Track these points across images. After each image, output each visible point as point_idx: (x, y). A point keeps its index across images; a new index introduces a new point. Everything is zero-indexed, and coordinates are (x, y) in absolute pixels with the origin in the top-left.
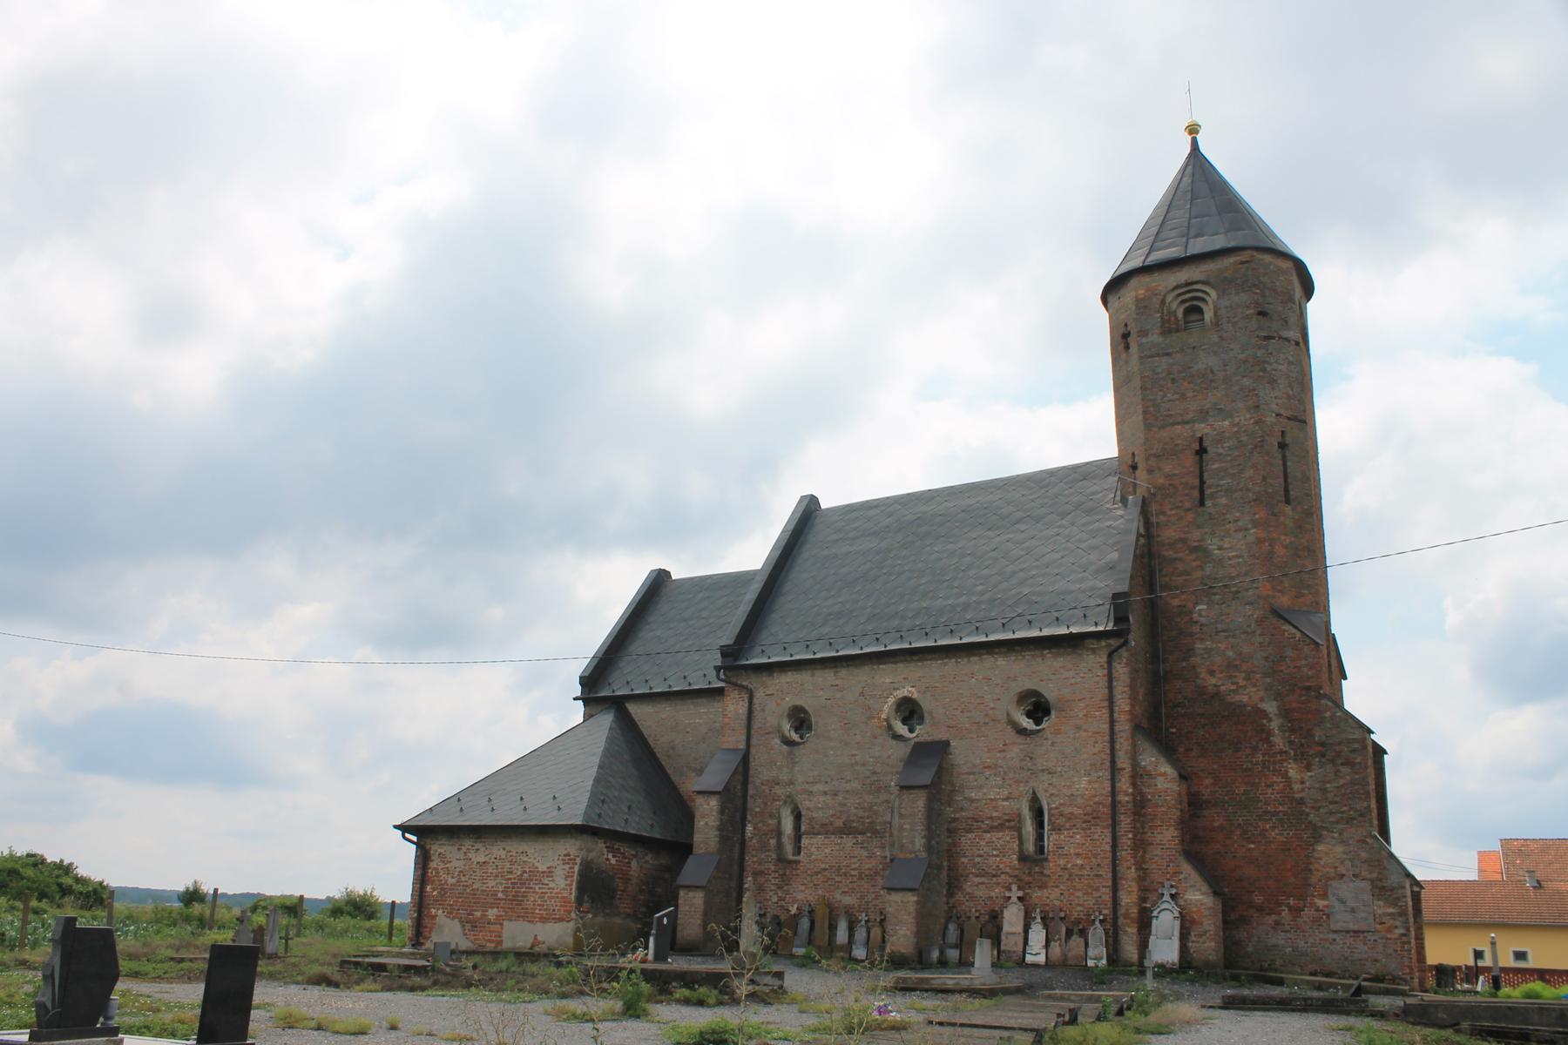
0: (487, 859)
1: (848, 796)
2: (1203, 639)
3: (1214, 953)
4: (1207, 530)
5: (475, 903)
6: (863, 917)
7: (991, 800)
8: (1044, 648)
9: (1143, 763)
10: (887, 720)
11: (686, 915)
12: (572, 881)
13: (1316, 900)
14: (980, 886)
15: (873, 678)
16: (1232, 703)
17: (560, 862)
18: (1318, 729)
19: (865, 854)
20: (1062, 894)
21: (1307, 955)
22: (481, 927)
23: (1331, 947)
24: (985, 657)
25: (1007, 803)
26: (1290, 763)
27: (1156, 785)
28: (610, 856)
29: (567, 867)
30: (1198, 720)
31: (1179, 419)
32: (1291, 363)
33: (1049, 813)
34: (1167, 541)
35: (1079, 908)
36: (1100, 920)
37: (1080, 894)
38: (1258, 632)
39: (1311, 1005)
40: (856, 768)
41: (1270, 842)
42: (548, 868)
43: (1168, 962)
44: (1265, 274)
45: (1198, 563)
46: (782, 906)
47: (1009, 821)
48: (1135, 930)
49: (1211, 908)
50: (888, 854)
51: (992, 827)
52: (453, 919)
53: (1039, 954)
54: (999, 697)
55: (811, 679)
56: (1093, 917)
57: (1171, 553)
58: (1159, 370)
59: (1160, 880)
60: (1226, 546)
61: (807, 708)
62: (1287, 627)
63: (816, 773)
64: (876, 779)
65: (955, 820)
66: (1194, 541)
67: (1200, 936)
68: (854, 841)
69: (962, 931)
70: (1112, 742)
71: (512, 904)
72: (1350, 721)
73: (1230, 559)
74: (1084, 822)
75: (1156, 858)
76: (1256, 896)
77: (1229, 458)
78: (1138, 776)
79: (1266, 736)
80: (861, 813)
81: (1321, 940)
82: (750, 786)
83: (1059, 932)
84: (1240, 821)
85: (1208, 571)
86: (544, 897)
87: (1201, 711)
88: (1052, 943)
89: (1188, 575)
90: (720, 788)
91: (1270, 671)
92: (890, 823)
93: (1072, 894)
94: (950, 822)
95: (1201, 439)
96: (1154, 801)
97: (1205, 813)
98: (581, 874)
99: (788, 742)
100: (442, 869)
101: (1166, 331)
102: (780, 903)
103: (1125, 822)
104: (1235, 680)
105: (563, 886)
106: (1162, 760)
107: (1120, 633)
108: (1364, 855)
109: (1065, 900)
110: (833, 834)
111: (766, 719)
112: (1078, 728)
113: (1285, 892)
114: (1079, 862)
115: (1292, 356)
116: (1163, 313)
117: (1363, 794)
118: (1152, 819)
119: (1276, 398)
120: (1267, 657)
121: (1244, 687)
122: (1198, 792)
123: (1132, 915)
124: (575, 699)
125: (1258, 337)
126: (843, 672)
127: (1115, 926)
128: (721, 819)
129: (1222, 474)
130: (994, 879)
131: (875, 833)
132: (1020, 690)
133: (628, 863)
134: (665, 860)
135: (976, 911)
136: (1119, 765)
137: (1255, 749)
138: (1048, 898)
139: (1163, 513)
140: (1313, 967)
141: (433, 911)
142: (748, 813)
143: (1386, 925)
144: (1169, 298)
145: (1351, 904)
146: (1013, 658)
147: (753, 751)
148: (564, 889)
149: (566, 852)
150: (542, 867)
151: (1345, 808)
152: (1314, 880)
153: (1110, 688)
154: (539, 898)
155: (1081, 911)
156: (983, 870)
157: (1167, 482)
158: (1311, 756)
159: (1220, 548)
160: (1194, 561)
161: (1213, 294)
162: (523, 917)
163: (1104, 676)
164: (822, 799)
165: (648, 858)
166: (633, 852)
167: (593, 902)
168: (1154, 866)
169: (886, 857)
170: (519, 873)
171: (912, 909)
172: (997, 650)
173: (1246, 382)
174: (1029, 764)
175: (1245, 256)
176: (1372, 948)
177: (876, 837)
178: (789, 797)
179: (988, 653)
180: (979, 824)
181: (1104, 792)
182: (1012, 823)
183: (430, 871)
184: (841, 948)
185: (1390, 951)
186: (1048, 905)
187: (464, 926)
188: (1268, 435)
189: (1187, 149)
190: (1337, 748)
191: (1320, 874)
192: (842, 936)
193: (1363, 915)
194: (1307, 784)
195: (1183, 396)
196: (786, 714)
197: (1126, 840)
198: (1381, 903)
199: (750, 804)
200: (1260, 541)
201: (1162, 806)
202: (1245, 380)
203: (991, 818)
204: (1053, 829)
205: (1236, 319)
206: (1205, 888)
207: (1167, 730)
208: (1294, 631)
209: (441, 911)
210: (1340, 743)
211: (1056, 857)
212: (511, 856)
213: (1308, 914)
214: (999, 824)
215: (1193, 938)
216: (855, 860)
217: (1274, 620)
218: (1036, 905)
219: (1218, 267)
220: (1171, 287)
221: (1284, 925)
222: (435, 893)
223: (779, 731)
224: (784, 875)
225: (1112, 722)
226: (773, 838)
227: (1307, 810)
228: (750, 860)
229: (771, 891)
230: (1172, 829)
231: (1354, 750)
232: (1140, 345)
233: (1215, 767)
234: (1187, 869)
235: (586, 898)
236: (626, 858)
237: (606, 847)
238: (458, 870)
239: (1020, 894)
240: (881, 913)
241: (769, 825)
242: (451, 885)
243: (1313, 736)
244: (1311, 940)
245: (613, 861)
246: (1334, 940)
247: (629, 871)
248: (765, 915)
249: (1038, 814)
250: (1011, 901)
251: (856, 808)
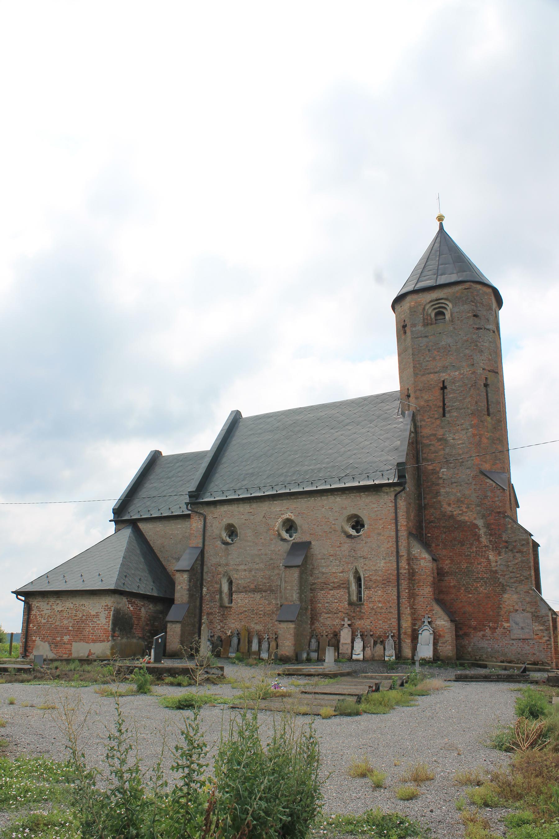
0: (63, 609)
1: (257, 572)
2: (444, 487)
3: (451, 652)
4: (446, 429)
5: (56, 633)
6: (266, 636)
7: (334, 573)
8: (362, 492)
9: (413, 553)
10: (278, 531)
11: (171, 637)
12: (109, 620)
13: (504, 623)
15: (270, 508)
16: (460, 521)
17: (103, 610)
18: (504, 534)
19: (267, 603)
20: (371, 622)
21: (499, 652)
22: (60, 646)
23: (512, 647)
24: (329, 497)
25: (341, 574)
26: (490, 552)
27: (420, 564)
28: (130, 606)
29: (107, 612)
30: (442, 529)
31: (432, 371)
32: (490, 342)
33: (364, 579)
34: (425, 435)
35: (380, 630)
37: (381, 622)
38: (474, 483)
39: (501, 678)
40: (262, 557)
41: (480, 593)
42: (96, 613)
43: (427, 657)
44: (477, 295)
45: (442, 447)
46: (223, 631)
47: (342, 584)
48: (410, 641)
49: (449, 628)
50: (279, 602)
51: (334, 588)
52: (45, 642)
54: (337, 518)
55: (237, 509)
56: (388, 634)
57: (428, 441)
58: (421, 345)
59: (423, 614)
60: (456, 438)
61: (235, 525)
62: (488, 480)
63: (240, 559)
64: (272, 562)
65: (314, 584)
66: (440, 435)
67: (444, 643)
68: (261, 596)
69: (319, 643)
70: (397, 542)
71: (77, 633)
72: (521, 529)
73: (458, 445)
74: (383, 584)
75: (421, 603)
76: (473, 621)
77: (458, 392)
78: (410, 559)
79: (477, 537)
80: (265, 581)
81: (506, 644)
82: (205, 567)
83: (370, 642)
84: (464, 583)
85: (447, 450)
86: (94, 629)
87: (443, 525)
88: (366, 649)
89: (437, 453)
90: (189, 568)
91: (479, 503)
92: (280, 586)
93: (376, 622)
94: (311, 585)
95: (443, 382)
96: (419, 573)
97: (446, 578)
98: (114, 615)
99: (226, 543)
100: (39, 615)
101: (426, 325)
102: (222, 630)
103: (404, 584)
104: (461, 508)
105: (104, 623)
106: (424, 550)
107: (401, 484)
108: (528, 599)
110: (249, 592)
111: (213, 530)
112: (379, 534)
113: (488, 620)
114: (380, 605)
115: (491, 338)
116: (424, 315)
117: (527, 568)
118: (419, 582)
119: (482, 360)
120: (478, 496)
121: (466, 512)
122: (443, 567)
123: (408, 633)
124: (110, 521)
125: (473, 328)
126: (254, 505)
127: (399, 638)
128: (190, 585)
129: (455, 400)
131: (272, 591)
132: (349, 514)
133: (139, 609)
134: (159, 607)
135: (326, 632)
136: (401, 554)
137: (472, 544)
139: (424, 421)
140: (502, 658)
141: (34, 638)
142: (204, 581)
143: (539, 635)
144: (427, 307)
145: (521, 625)
146: (344, 497)
147: (206, 548)
148: (105, 624)
149: (106, 604)
150: (93, 613)
151: (518, 575)
152: (502, 613)
153: (396, 513)
154: (92, 629)
155: (381, 631)
156: (330, 610)
157: (426, 404)
158: (501, 548)
159: (453, 439)
160: (440, 445)
161: (450, 305)
162: (83, 640)
163: (393, 506)
164: (243, 573)
165: (151, 606)
166: (142, 604)
167: (120, 631)
168: (420, 607)
169: (278, 604)
170: (80, 616)
171: (292, 632)
172: (336, 493)
173: (467, 351)
174: (354, 554)
175: (467, 285)
176: (532, 648)
177: (273, 594)
178: (225, 572)
179: (331, 495)
180: (327, 585)
181: (393, 568)
182: (345, 585)
183: (32, 616)
184: (255, 653)
185: (541, 649)
186: (364, 628)
187: (50, 646)
188: (478, 380)
189: (437, 229)
190: (514, 544)
191: (506, 609)
192: (255, 646)
193: (527, 630)
194: (499, 563)
195: (434, 359)
196: (224, 528)
197: (405, 594)
198: (537, 624)
199: (205, 576)
200: (474, 435)
201: (424, 575)
202: (467, 350)
203: (333, 582)
204: (366, 588)
205: (462, 319)
206: (446, 618)
207: (426, 535)
208: (491, 482)
209: (38, 638)
210: (515, 541)
211: (368, 603)
212: (76, 607)
213: (499, 631)
214: (338, 586)
215: (440, 644)
216: (261, 606)
217: (482, 477)
219: (453, 291)
220: (428, 301)
221: (487, 636)
222: (35, 628)
223: (220, 537)
224: (224, 614)
225: (397, 531)
226: (217, 595)
227: (499, 576)
228: (205, 607)
229: (217, 623)
230: (429, 587)
231: (523, 545)
232: (412, 332)
233: (451, 554)
234: (437, 609)
235: (117, 629)
236: (138, 607)
237: (128, 601)
238: (47, 615)
239: (349, 622)
240: (276, 634)
241: (215, 588)
242: (44, 623)
243: (501, 537)
244: (501, 644)
245: (131, 609)
246: (513, 644)
247: (140, 614)
248: (213, 636)
249: (358, 580)
251: (261, 578)
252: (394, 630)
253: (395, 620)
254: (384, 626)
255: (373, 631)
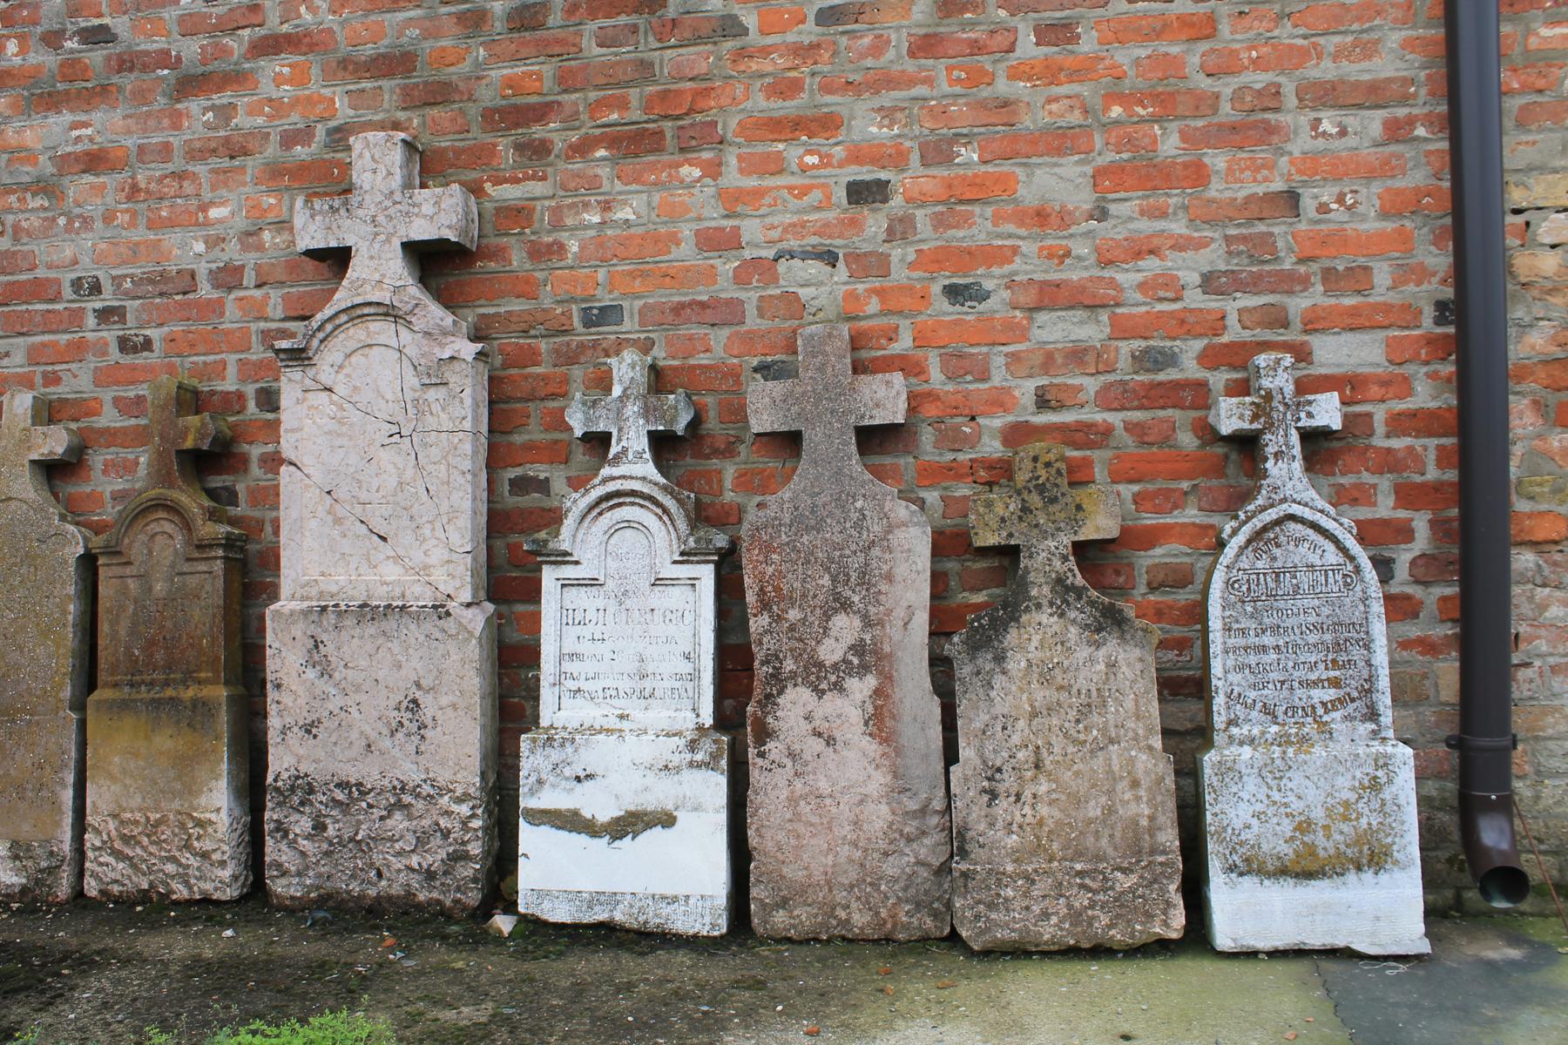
14: (78, 186)
20: (862, 193)
35: (1056, 329)
36: (1314, 440)
53: (667, 820)
56: (1230, 417)
109: (899, 255)
130: (198, 112)
135: (48, 413)
138: (718, 242)
155: (1078, 355)
186: (724, 313)
218: (608, 314)
250: (343, 297)
252: (1355, 322)
253: (1373, 122)
254: (1141, 249)
255: (909, 366)
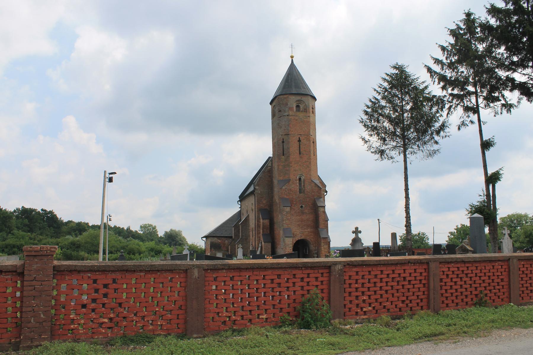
245: (220, 241)
